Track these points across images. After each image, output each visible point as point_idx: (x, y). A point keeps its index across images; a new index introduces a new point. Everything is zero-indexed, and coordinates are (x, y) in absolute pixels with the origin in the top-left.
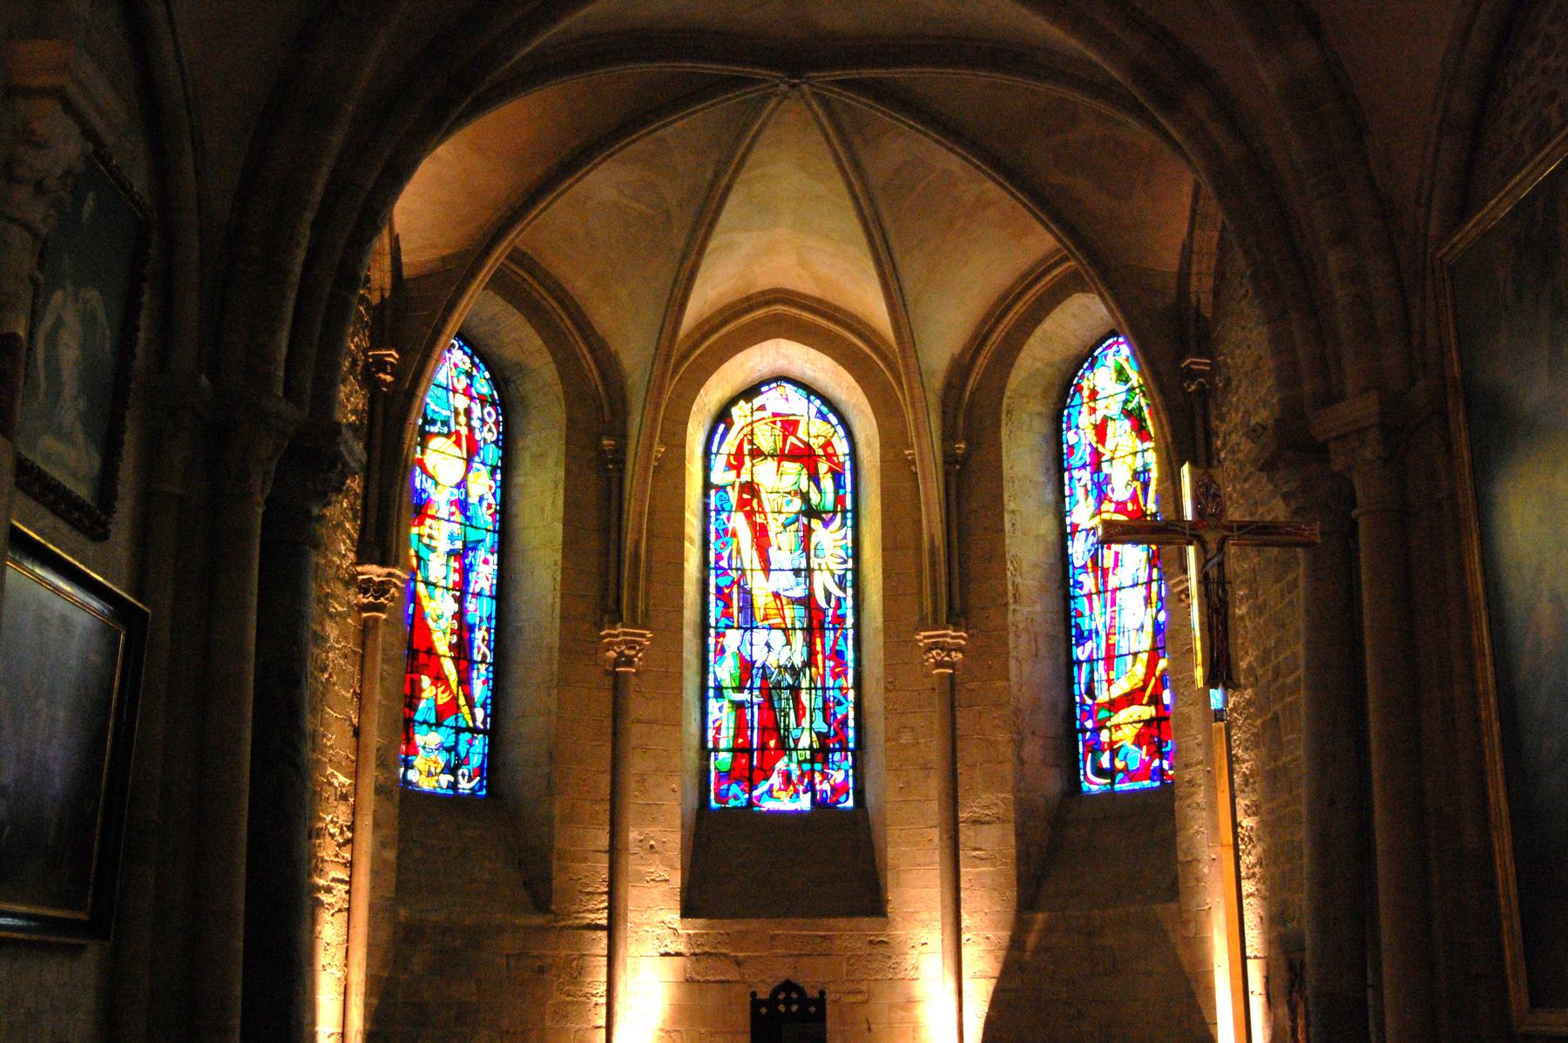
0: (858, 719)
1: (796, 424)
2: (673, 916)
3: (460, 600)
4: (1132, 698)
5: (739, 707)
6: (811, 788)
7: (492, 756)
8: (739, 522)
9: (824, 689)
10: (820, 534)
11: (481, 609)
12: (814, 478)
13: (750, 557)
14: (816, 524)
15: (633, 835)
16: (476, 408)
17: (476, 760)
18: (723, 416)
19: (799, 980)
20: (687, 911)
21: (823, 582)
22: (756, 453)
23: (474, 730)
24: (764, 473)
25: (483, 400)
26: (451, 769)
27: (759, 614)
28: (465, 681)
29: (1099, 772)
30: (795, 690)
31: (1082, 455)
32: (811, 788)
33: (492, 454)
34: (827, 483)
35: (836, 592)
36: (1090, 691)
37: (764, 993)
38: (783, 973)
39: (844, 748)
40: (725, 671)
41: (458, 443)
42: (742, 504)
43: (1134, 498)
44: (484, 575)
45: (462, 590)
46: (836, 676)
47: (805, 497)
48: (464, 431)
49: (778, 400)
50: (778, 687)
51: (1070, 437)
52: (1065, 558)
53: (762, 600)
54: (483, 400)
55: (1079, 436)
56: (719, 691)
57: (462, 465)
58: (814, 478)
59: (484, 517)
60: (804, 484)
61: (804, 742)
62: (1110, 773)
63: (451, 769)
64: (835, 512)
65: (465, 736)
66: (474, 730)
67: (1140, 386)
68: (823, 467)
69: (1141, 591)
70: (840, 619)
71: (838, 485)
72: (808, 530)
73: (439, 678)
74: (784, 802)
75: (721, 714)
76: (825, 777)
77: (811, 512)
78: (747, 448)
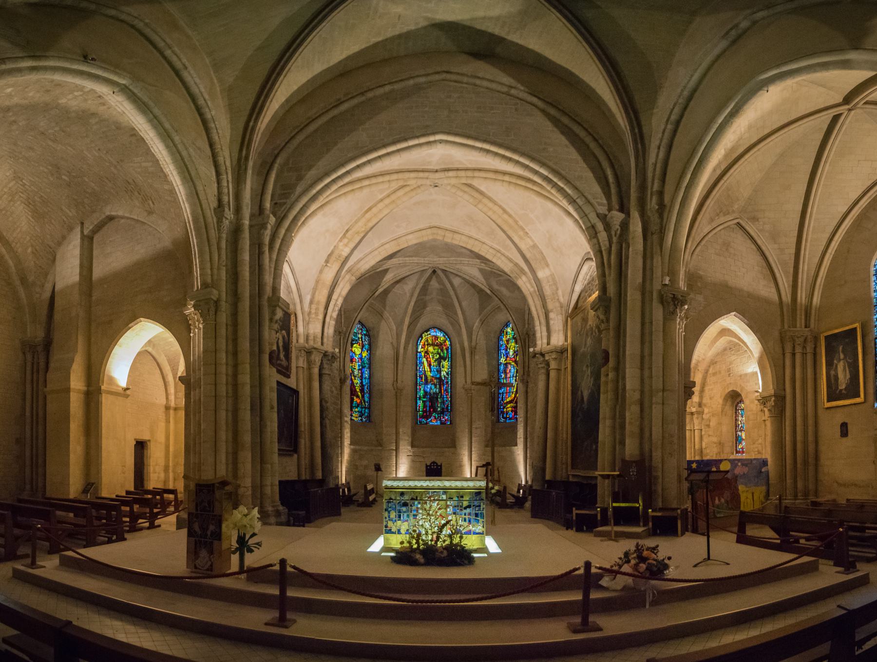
0: (451, 405)
1: (438, 338)
2: (409, 448)
3: (362, 380)
4: (510, 402)
5: (423, 401)
6: (440, 420)
7: (369, 413)
8: (424, 360)
9: (443, 398)
11: (365, 382)
12: (442, 350)
13: (427, 368)
14: (442, 360)
15: (401, 430)
16: (363, 337)
17: (366, 414)
18: (421, 336)
19: (437, 461)
20: (412, 446)
21: (443, 373)
23: (365, 408)
24: (431, 349)
25: (365, 335)
26: (361, 416)
27: (429, 381)
28: (363, 396)
29: (503, 417)
30: (437, 398)
31: (504, 346)
32: (440, 420)
33: (367, 347)
35: (447, 376)
36: (502, 400)
37: (428, 464)
38: (433, 460)
39: (448, 411)
40: (422, 393)
41: (359, 345)
42: (425, 356)
43: (514, 357)
44: (366, 374)
45: (362, 378)
46: (446, 395)
47: (439, 354)
48: (361, 342)
49: (433, 333)
50: (433, 397)
51: (501, 343)
52: (499, 370)
53: (429, 378)
54: (365, 335)
56: (420, 399)
57: (360, 350)
58: (442, 350)
59: (366, 361)
60: (440, 351)
61: (439, 409)
62: (506, 418)
63: (361, 416)
64: (446, 358)
65: (363, 409)
66: (365, 408)
67: (514, 338)
68: (444, 348)
69: (515, 378)
70: (447, 382)
71: (447, 352)
72: (440, 362)
73: (358, 397)
74: (434, 423)
75: (420, 403)
76: (443, 418)
77: (441, 358)
78: (426, 343)
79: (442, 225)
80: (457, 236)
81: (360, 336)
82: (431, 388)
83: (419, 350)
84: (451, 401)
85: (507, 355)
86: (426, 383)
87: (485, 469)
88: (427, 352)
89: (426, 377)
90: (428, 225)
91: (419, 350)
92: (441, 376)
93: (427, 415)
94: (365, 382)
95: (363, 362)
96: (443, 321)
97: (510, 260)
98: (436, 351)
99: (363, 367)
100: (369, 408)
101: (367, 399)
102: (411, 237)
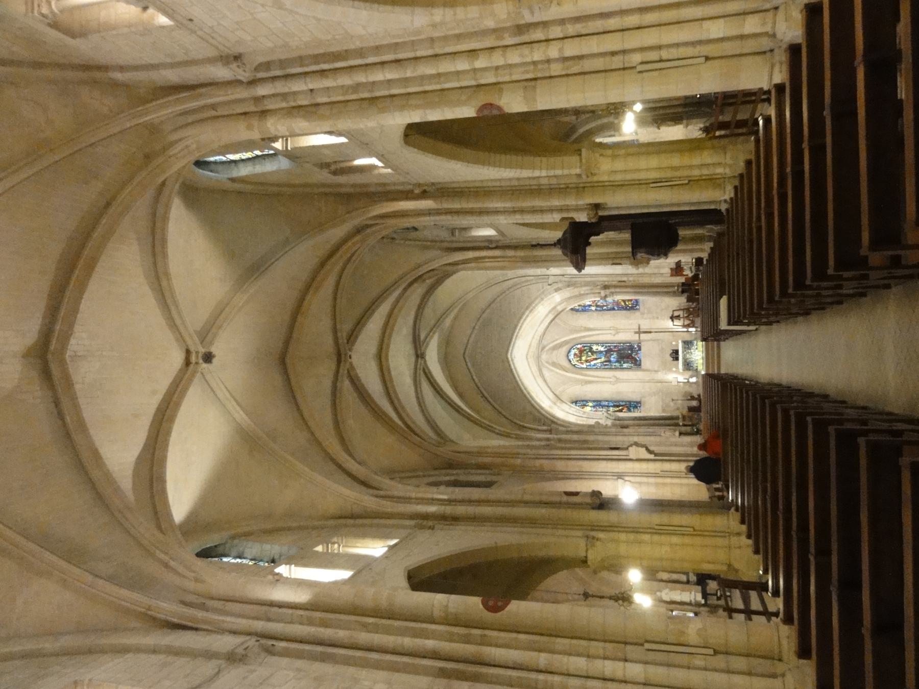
8: (592, 363)
13: (599, 361)
18: (574, 365)
21: (602, 349)
24: (584, 358)
49: (571, 357)
55: (580, 308)
62: (636, 305)
75: (625, 365)
79: (526, 353)
80: (533, 344)
83: (584, 366)
85: (590, 306)
86: (609, 361)
87: (675, 320)
88: (587, 361)
89: (606, 362)
90: (525, 361)
95: (597, 405)
96: (564, 349)
97: (547, 315)
100: (630, 402)
101: (624, 403)
102: (533, 369)
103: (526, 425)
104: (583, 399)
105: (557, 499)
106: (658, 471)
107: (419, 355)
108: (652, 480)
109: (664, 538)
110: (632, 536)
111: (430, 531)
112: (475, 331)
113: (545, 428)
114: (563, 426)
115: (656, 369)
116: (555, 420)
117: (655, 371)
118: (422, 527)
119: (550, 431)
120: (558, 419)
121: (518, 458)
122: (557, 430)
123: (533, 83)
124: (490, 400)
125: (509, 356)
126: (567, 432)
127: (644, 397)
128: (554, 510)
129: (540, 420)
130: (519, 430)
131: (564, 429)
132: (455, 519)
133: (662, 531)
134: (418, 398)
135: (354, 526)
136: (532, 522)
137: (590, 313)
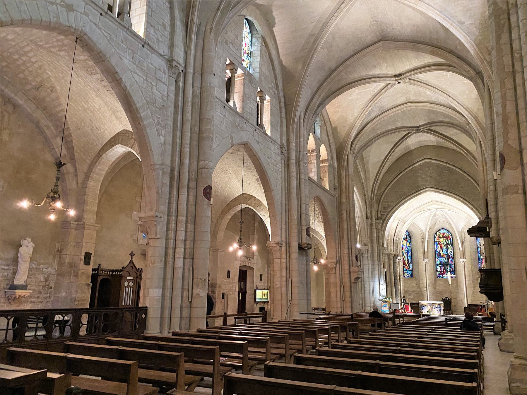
2: (434, 290)
8: (439, 246)
10: (449, 246)
11: (409, 258)
13: (440, 250)
18: (436, 233)
21: (449, 252)
22: (440, 237)
24: (442, 240)
25: (408, 235)
28: (409, 265)
30: (447, 265)
33: (409, 241)
34: (449, 241)
40: (438, 262)
44: (410, 255)
49: (442, 231)
50: (445, 264)
53: (442, 255)
54: (408, 235)
59: (409, 248)
71: (450, 241)
73: (406, 265)
75: (438, 268)
77: (447, 244)
81: (405, 236)
82: (444, 260)
83: (436, 241)
84: (454, 266)
86: (441, 257)
89: (440, 254)
90: (431, 200)
91: (436, 241)
92: (448, 254)
93: (442, 273)
94: (409, 258)
98: (444, 241)
99: (408, 251)
100: (412, 271)
103: (381, 203)
104: (412, 240)
105: (304, 223)
106: (344, 284)
107: (418, 129)
108: (338, 280)
109: (284, 283)
110: (284, 266)
111: (280, 152)
112: (445, 164)
113: (379, 215)
114: (381, 228)
115: (437, 288)
116: (385, 222)
117: (435, 287)
118: (282, 147)
119: (378, 218)
120: (387, 224)
121: (346, 200)
122: (379, 223)
123: (520, 191)
124: (397, 178)
125: (428, 189)
126: (377, 229)
127: (416, 279)
128: (296, 222)
129: (385, 212)
130: (377, 199)
131: (380, 228)
132: (288, 166)
133: (288, 283)
134: (387, 131)
135: (280, 108)
136: (288, 211)
137: (475, 243)
